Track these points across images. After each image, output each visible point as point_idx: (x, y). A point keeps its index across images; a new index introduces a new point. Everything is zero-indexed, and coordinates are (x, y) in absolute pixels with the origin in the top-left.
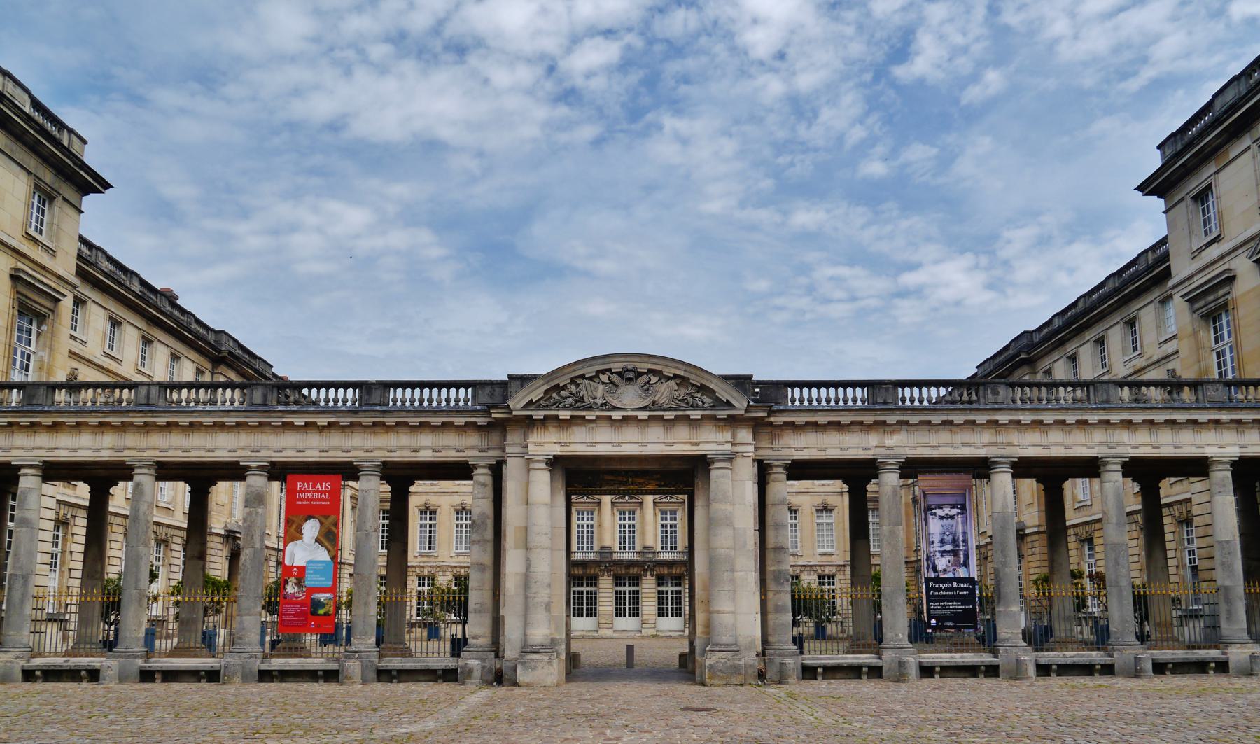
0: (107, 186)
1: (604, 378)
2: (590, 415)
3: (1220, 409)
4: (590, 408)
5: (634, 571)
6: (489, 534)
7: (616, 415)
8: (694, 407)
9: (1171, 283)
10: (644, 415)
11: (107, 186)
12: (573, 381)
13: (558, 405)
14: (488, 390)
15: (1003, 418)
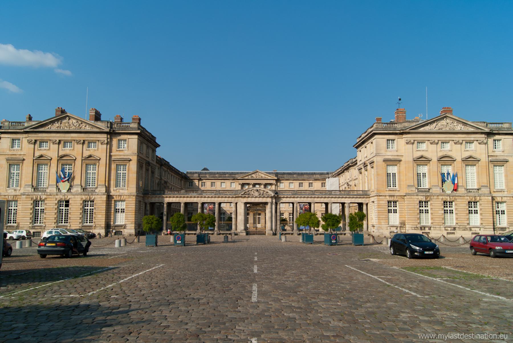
0: (159, 146)
1: (253, 191)
2: (251, 196)
3: (347, 195)
4: (250, 195)
5: (259, 212)
6: (235, 213)
7: (254, 196)
8: (266, 195)
9: (357, 165)
10: (259, 196)
11: (159, 146)
12: (248, 191)
13: (246, 195)
14: (235, 191)
15: (313, 196)
